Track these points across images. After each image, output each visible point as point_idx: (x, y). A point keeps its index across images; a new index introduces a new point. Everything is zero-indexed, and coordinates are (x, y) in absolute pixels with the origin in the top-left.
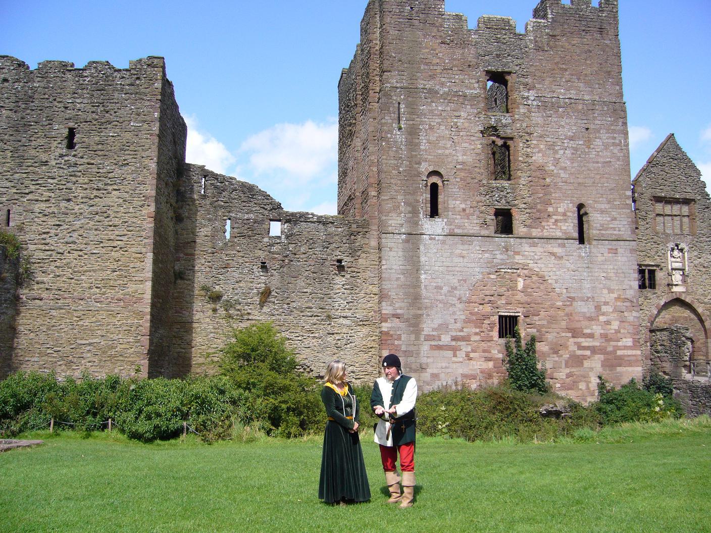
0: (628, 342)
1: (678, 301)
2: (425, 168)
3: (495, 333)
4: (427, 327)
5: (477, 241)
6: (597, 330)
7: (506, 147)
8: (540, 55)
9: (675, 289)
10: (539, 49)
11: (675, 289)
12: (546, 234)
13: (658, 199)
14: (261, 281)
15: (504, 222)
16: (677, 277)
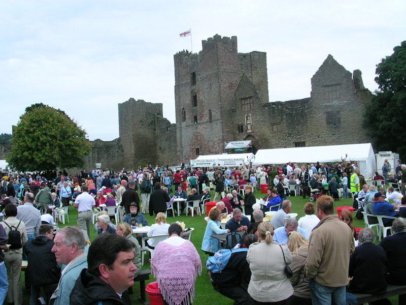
2: (182, 108)
3: (195, 154)
5: (191, 127)
7: (196, 96)
9: (248, 131)
10: (201, 61)
11: (248, 131)
12: (203, 121)
15: (196, 118)
16: (249, 127)
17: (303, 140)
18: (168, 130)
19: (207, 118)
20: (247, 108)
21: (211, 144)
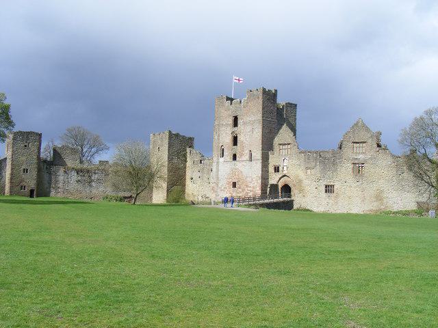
0: (258, 189)
1: (285, 176)
4: (220, 185)
6: (252, 185)
8: (245, 109)
13: (280, 144)
14: (199, 174)
15: (235, 157)
16: (285, 168)
17: (332, 184)
18: (201, 163)
19: (247, 157)
20: (284, 152)
21: (249, 179)
